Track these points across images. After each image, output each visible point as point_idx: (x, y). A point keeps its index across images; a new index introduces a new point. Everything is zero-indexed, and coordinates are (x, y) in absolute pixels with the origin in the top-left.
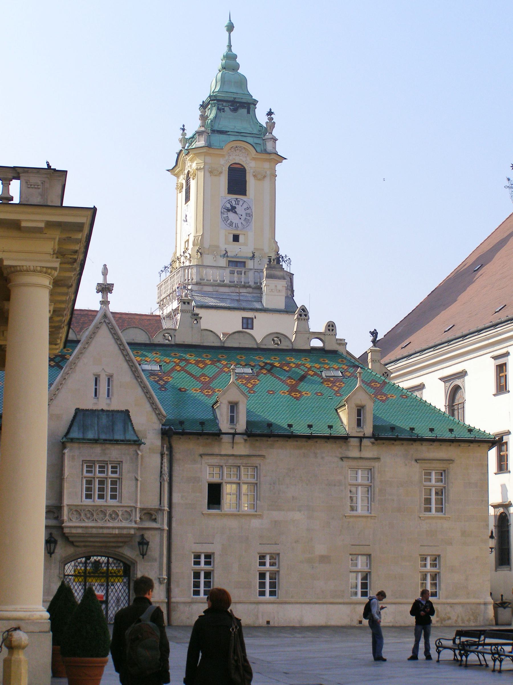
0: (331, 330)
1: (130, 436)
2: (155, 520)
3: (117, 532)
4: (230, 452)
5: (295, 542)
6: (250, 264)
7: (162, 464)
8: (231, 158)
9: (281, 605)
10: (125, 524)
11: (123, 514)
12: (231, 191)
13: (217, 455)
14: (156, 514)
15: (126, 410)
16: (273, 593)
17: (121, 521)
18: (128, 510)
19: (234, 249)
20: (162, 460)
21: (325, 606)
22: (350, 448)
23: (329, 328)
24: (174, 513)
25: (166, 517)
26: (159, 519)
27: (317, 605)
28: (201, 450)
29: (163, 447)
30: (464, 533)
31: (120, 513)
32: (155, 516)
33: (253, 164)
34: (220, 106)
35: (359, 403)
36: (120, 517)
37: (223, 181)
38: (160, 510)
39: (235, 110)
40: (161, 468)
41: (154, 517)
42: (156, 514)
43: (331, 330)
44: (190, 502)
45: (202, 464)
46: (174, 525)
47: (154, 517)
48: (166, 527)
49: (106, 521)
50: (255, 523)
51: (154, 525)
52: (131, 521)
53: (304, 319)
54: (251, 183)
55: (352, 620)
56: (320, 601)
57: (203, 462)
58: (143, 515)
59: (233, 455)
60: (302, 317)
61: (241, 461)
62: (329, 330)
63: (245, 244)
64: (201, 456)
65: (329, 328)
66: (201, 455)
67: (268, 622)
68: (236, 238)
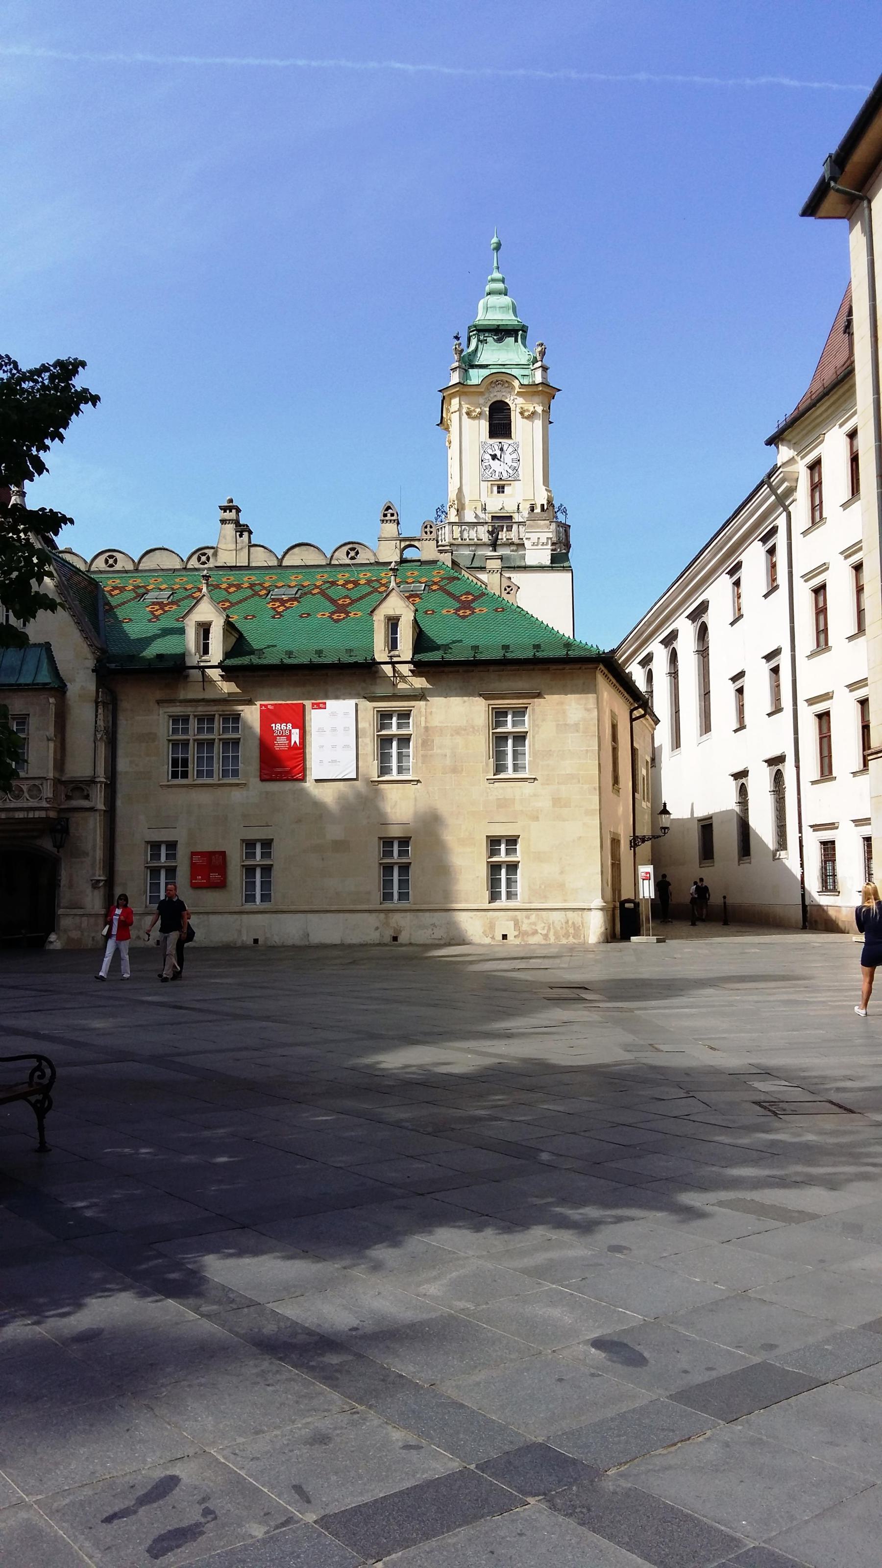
0: (429, 533)
1: (44, 677)
2: (87, 797)
3: (21, 815)
4: (200, 696)
5: (297, 822)
6: (517, 518)
7: (96, 716)
8: (492, 395)
9: (274, 915)
10: (33, 803)
11: (29, 790)
12: (493, 434)
13: (181, 701)
14: (87, 788)
15: (45, 643)
16: (265, 898)
17: (27, 800)
18: (37, 782)
19: (496, 504)
20: (97, 711)
21: (341, 915)
22: (378, 681)
23: (426, 530)
24: (119, 787)
25: (101, 792)
26: (93, 795)
27: (328, 915)
28: (159, 695)
29: (97, 692)
30: (557, 801)
31: (25, 788)
32: (88, 791)
33: (520, 400)
34: (482, 338)
35: (391, 613)
36: (26, 794)
37: (484, 425)
38: (92, 781)
39: (500, 340)
40: (96, 723)
41: (85, 793)
42: (87, 788)
43: (429, 533)
44: (142, 770)
45: (159, 715)
46: (119, 803)
47: (85, 793)
48: (101, 806)
49: (6, 800)
50: (237, 796)
51: (85, 803)
52: (41, 799)
53: (391, 521)
54: (518, 423)
55: (383, 936)
56: (334, 908)
57: (161, 712)
58: (71, 790)
59: (203, 700)
60: (387, 518)
61: (215, 708)
62: (426, 533)
63: (511, 496)
64: (158, 703)
65: (426, 530)
66: (159, 702)
67: (256, 941)
68: (501, 489)
